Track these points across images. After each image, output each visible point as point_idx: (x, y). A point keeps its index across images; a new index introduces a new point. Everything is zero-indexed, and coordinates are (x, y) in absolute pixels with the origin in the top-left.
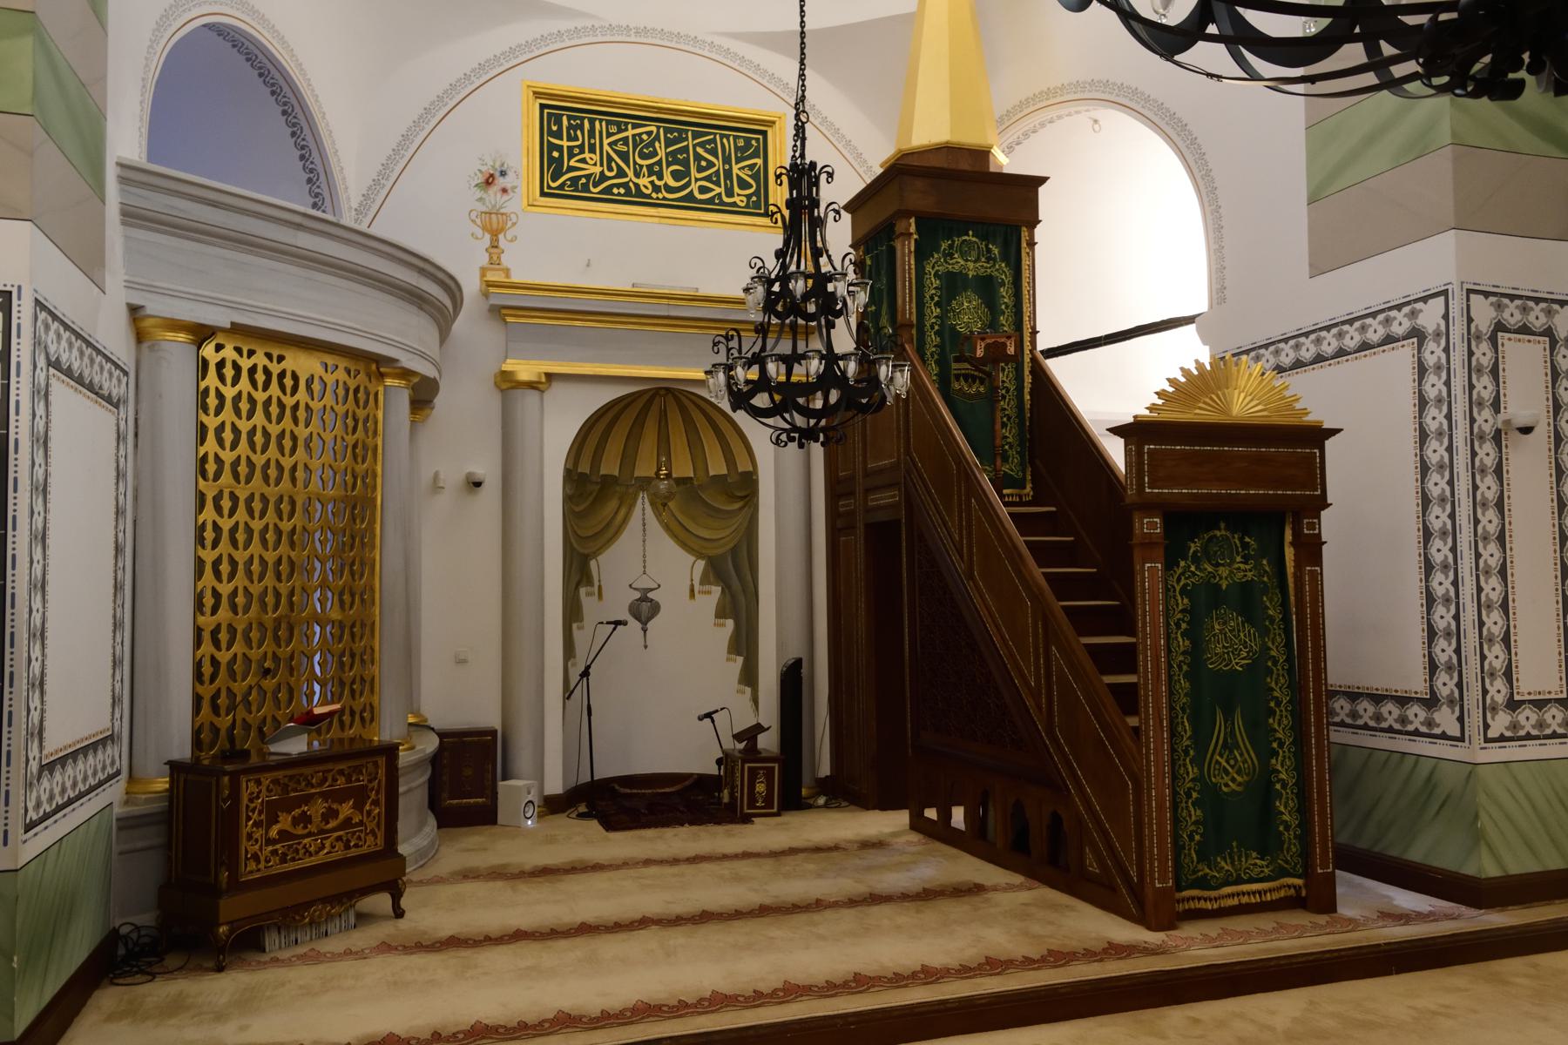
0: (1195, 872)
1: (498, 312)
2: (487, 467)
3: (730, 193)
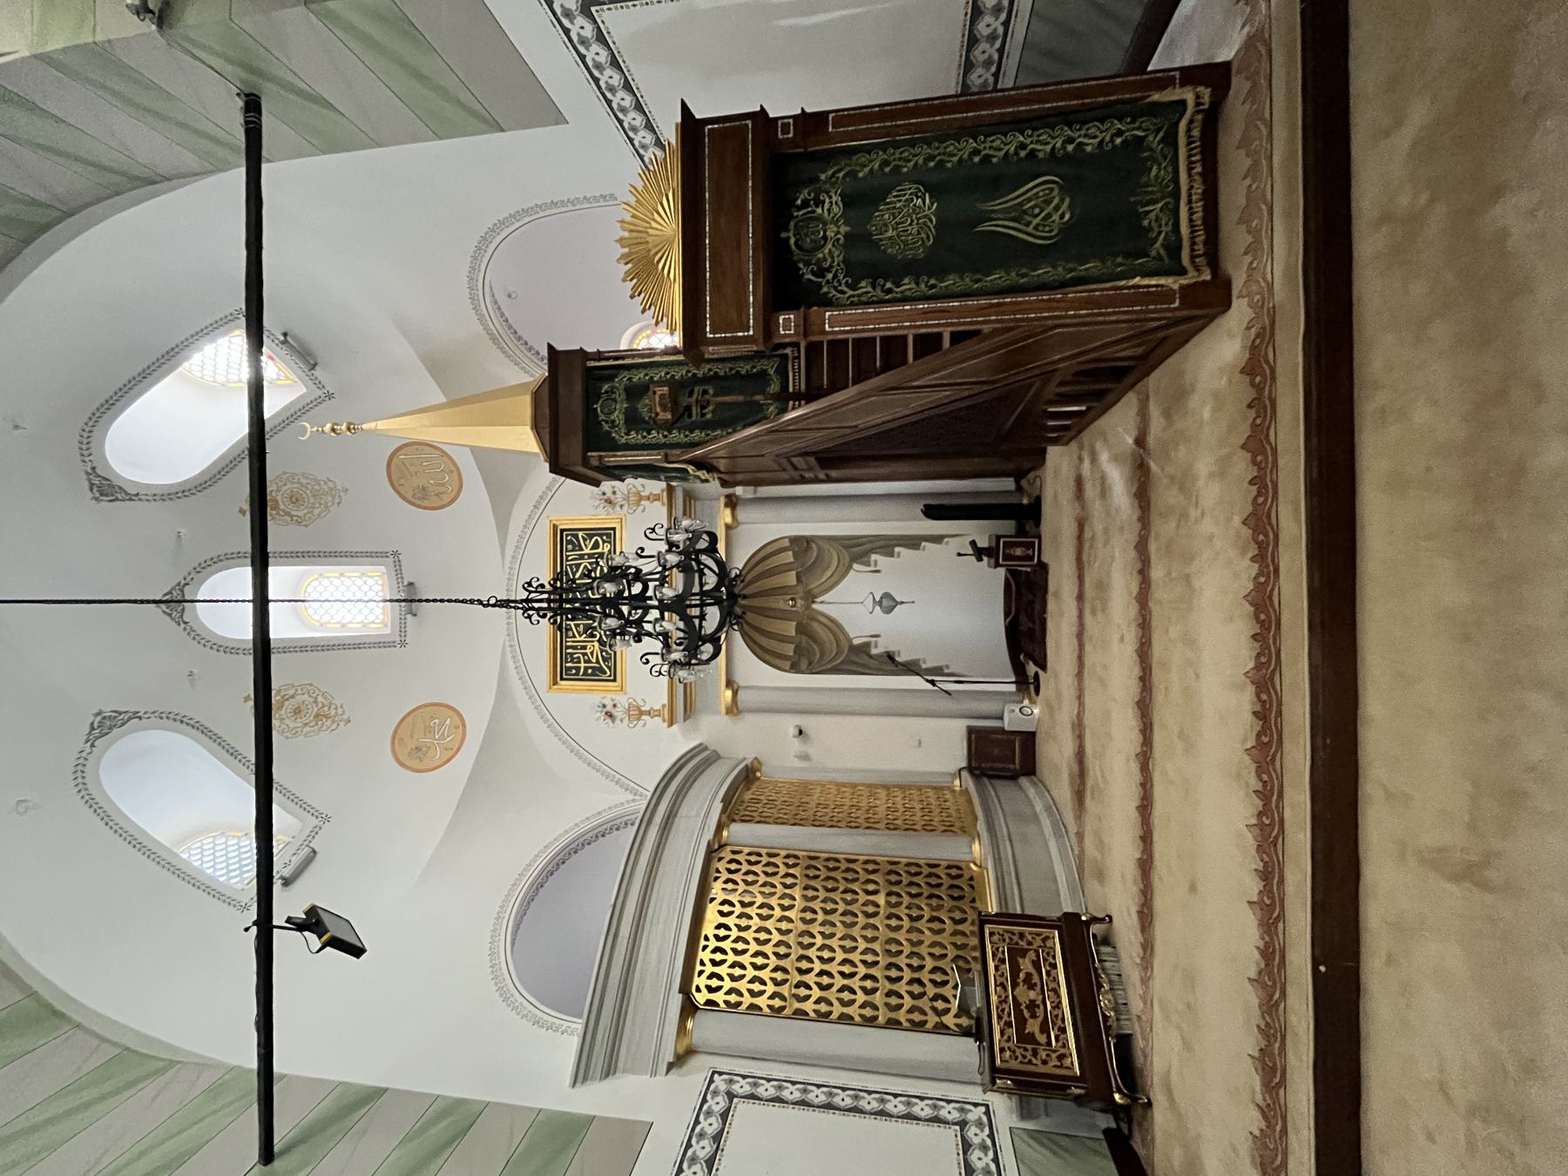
0: (1159, 258)
1: (689, 712)
2: (789, 724)
3: (601, 555)
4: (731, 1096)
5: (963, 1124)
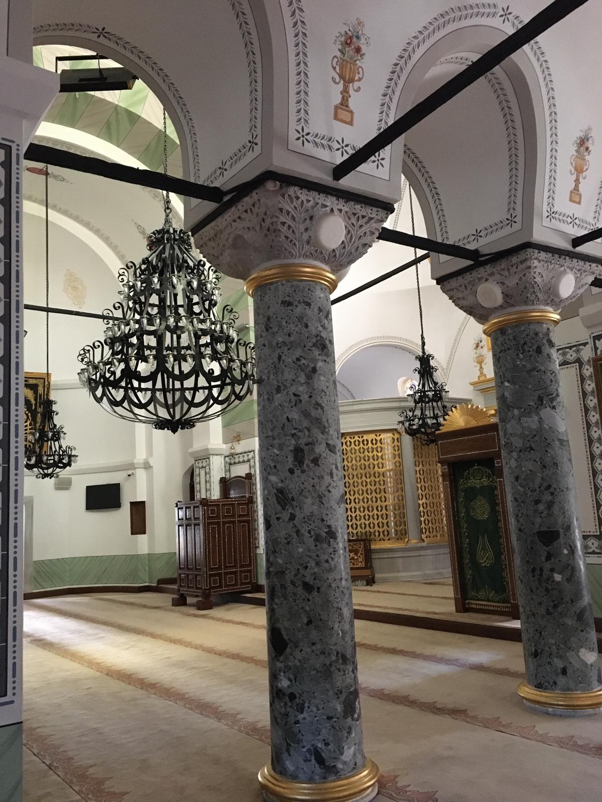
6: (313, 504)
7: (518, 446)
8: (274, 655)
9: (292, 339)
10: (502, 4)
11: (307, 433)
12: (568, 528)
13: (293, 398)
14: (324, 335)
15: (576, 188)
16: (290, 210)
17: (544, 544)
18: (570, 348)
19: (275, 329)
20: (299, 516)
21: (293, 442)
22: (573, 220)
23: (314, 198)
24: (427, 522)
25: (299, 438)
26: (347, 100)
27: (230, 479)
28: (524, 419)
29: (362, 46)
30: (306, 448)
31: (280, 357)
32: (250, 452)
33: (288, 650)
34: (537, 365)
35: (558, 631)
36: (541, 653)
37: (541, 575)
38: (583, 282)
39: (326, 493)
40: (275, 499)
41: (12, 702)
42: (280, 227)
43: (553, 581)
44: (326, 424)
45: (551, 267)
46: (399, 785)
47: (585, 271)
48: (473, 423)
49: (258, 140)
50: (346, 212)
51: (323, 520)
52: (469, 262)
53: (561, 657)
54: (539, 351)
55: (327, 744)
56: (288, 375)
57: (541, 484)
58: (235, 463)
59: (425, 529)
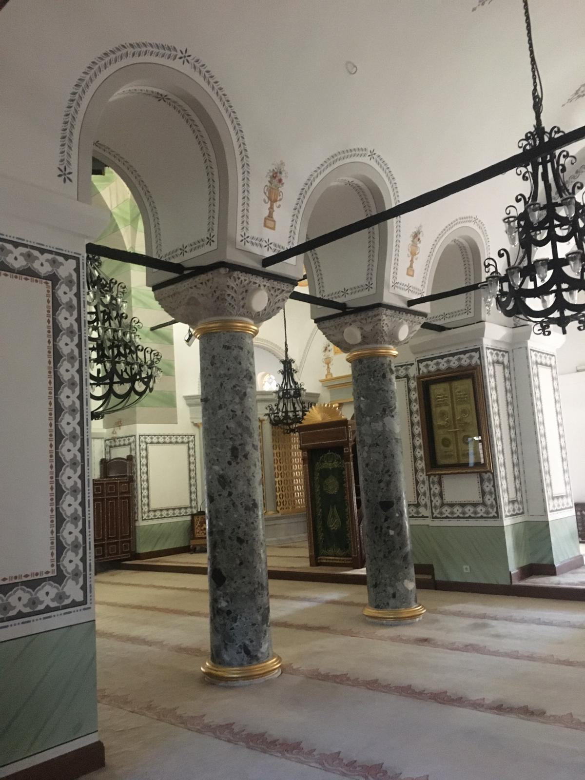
4: (188, 442)
5: (191, 507)
6: (243, 485)
7: (368, 442)
8: (215, 587)
9: (230, 372)
10: (370, 148)
11: (240, 437)
12: (399, 499)
13: (231, 413)
14: (251, 369)
15: (411, 266)
16: (234, 286)
17: (384, 510)
18: (402, 366)
19: (218, 365)
20: (235, 492)
21: (231, 443)
22: (408, 288)
23: (249, 278)
24: (281, 496)
25: (235, 440)
26: (272, 214)
27: (111, 460)
28: (373, 424)
29: (282, 178)
30: (239, 447)
31: (221, 385)
32: (131, 436)
33: (226, 582)
34: (383, 386)
35: (391, 568)
36: (379, 584)
37: (381, 531)
38: (413, 329)
39: (252, 478)
40: (217, 483)
41: (90, 608)
42: (227, 297)
43: (389, 535)
44: (252, 431)
45: (393, 320)
46: (294, 667)
47: (415, 322)
48: (329, 419)
49: (215, 239)
50: (268, 287)
51: (250, 496)
52: (340, 311)
53: (392, 586)
54: (384, 376)
55: (252, 642)
56: (228, 397)
57: (383, 469)
58: (115, 446)
59: (280, 502)
